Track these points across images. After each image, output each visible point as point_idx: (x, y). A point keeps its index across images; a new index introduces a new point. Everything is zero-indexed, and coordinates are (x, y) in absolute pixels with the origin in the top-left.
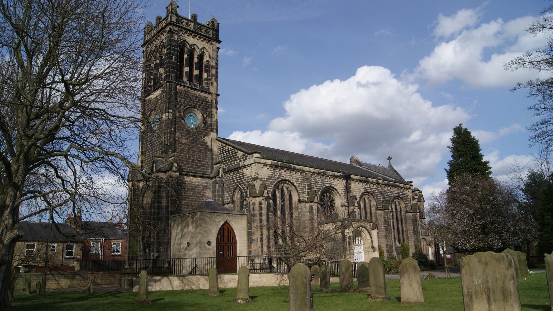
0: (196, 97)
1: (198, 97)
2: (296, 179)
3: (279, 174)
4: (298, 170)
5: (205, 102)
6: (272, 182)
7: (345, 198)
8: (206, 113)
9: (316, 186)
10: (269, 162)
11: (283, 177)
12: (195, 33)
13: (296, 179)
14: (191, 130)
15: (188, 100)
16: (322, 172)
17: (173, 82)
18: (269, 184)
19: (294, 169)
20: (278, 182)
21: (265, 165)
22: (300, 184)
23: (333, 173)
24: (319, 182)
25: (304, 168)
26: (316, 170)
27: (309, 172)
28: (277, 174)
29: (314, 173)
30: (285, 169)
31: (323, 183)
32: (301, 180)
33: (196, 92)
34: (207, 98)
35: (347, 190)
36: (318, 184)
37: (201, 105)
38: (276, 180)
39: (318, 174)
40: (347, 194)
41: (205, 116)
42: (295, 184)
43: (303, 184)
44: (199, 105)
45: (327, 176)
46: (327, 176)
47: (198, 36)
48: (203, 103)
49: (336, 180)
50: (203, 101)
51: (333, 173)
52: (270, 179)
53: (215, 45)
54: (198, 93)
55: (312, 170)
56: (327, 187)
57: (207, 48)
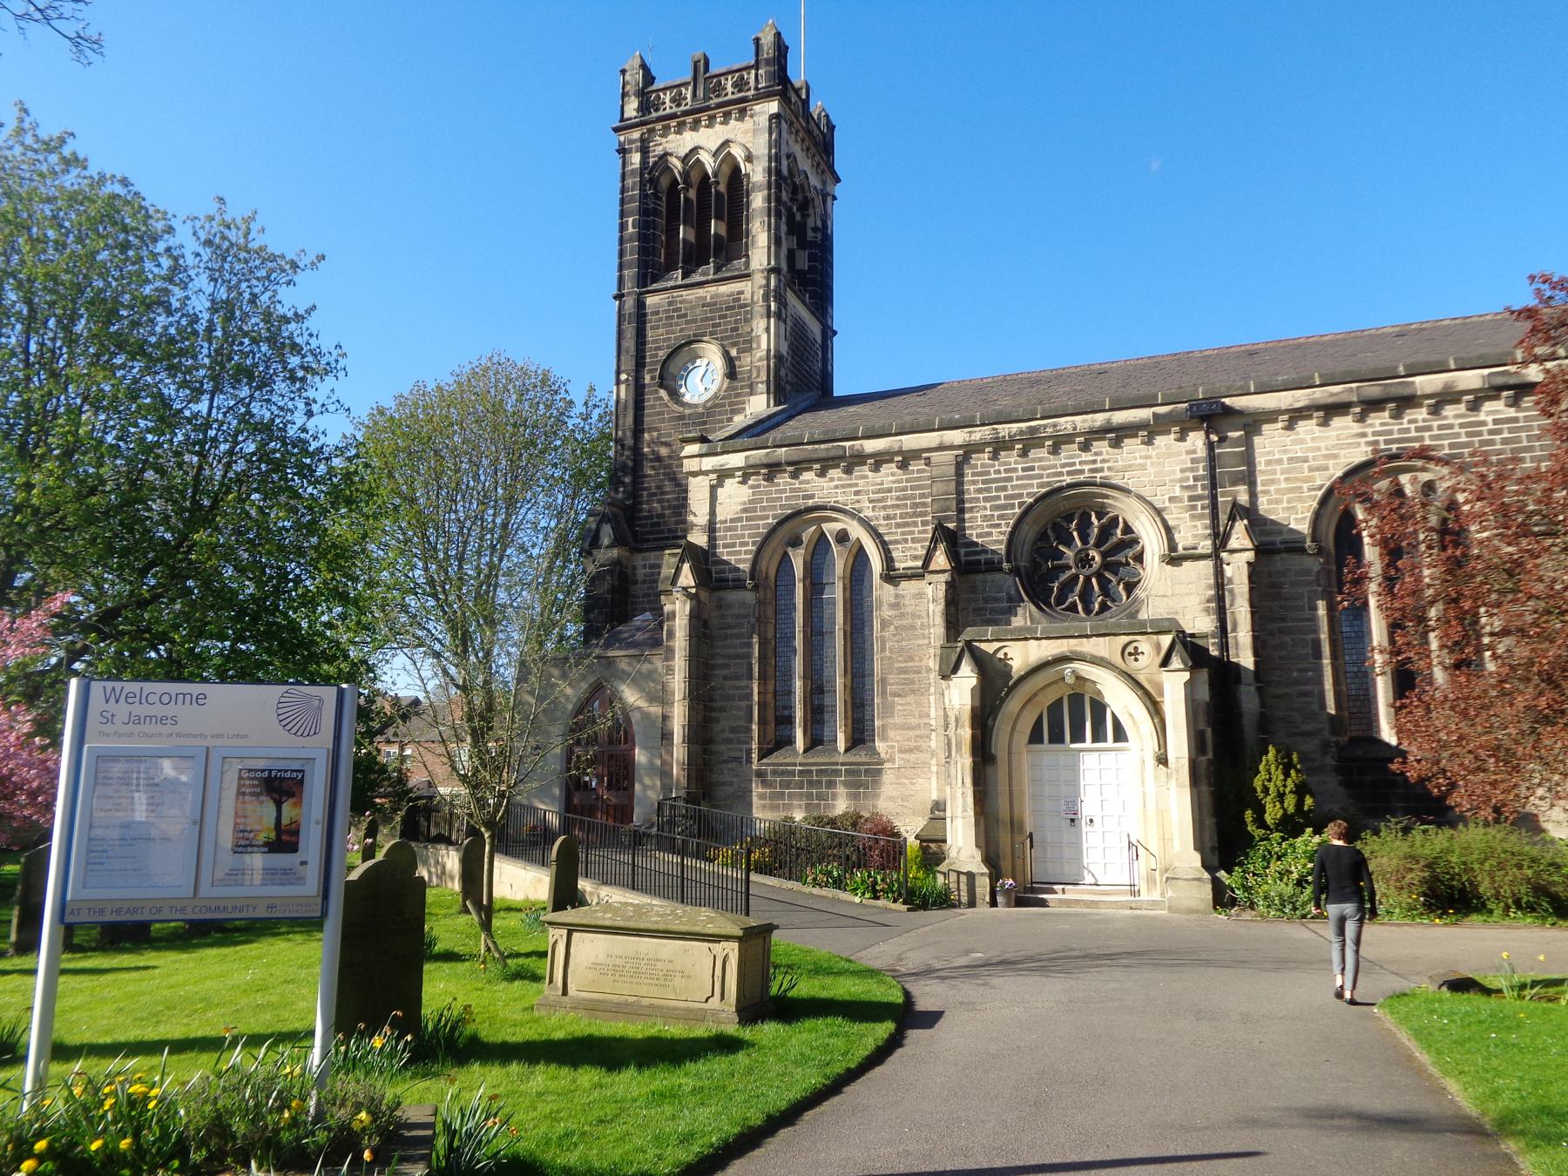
0: (703, 306)
1: (709, 305)
2: (879, 491)
3: (792, 490)
4: (879, 460)
5: (733, 308)
6: (758, 527)
7: (1193, 517)
8: (734, 344)
9: (986, 499)
10: (736, 460)
11: (811, 497)
12: (695, 116)
13: (879, 491)
14: (687, 412)
15: (677, 325)
16: (1021, 432)
17: (629, 294)
18: (743, 536)
19: (859, 459)
20: (781, 523)
21: (723, 475)
22: (898, 506)
23: (1099, 419)
24: (1010, 479)
25: (911, 442)
26: (980, 434)
27: (941, 448)
28: (784, 491)
29: (970, 450)
30: (817, 466)
31: (1041, 476)
32: (905, 489)
33: (700, 292)
34: (742, 292)
35: (1213, 477)
36: (1004, 488)
37: (719, 325)
38: (774, 517)
39: (999, 446)
40: (1214, 498)
41: (734, 353)
42: (868, 513)
43: (915, 505)
44: (714, 325)
45: (1068, 439)
46: (1059, 442)
47: (704, 117)
48: (725, 317)
49: (1132, 445)
50: (728, 309)
51: (1099, 419)
52: (748, 519)
53: (763, 113)
54: (707, 292)
55: (957, 437)
56: (1060, 489)
57: (740, 138)
